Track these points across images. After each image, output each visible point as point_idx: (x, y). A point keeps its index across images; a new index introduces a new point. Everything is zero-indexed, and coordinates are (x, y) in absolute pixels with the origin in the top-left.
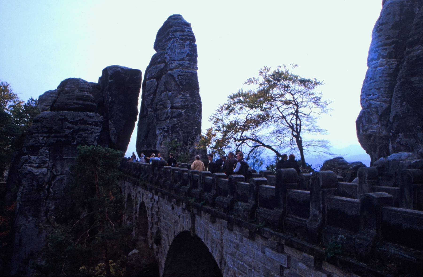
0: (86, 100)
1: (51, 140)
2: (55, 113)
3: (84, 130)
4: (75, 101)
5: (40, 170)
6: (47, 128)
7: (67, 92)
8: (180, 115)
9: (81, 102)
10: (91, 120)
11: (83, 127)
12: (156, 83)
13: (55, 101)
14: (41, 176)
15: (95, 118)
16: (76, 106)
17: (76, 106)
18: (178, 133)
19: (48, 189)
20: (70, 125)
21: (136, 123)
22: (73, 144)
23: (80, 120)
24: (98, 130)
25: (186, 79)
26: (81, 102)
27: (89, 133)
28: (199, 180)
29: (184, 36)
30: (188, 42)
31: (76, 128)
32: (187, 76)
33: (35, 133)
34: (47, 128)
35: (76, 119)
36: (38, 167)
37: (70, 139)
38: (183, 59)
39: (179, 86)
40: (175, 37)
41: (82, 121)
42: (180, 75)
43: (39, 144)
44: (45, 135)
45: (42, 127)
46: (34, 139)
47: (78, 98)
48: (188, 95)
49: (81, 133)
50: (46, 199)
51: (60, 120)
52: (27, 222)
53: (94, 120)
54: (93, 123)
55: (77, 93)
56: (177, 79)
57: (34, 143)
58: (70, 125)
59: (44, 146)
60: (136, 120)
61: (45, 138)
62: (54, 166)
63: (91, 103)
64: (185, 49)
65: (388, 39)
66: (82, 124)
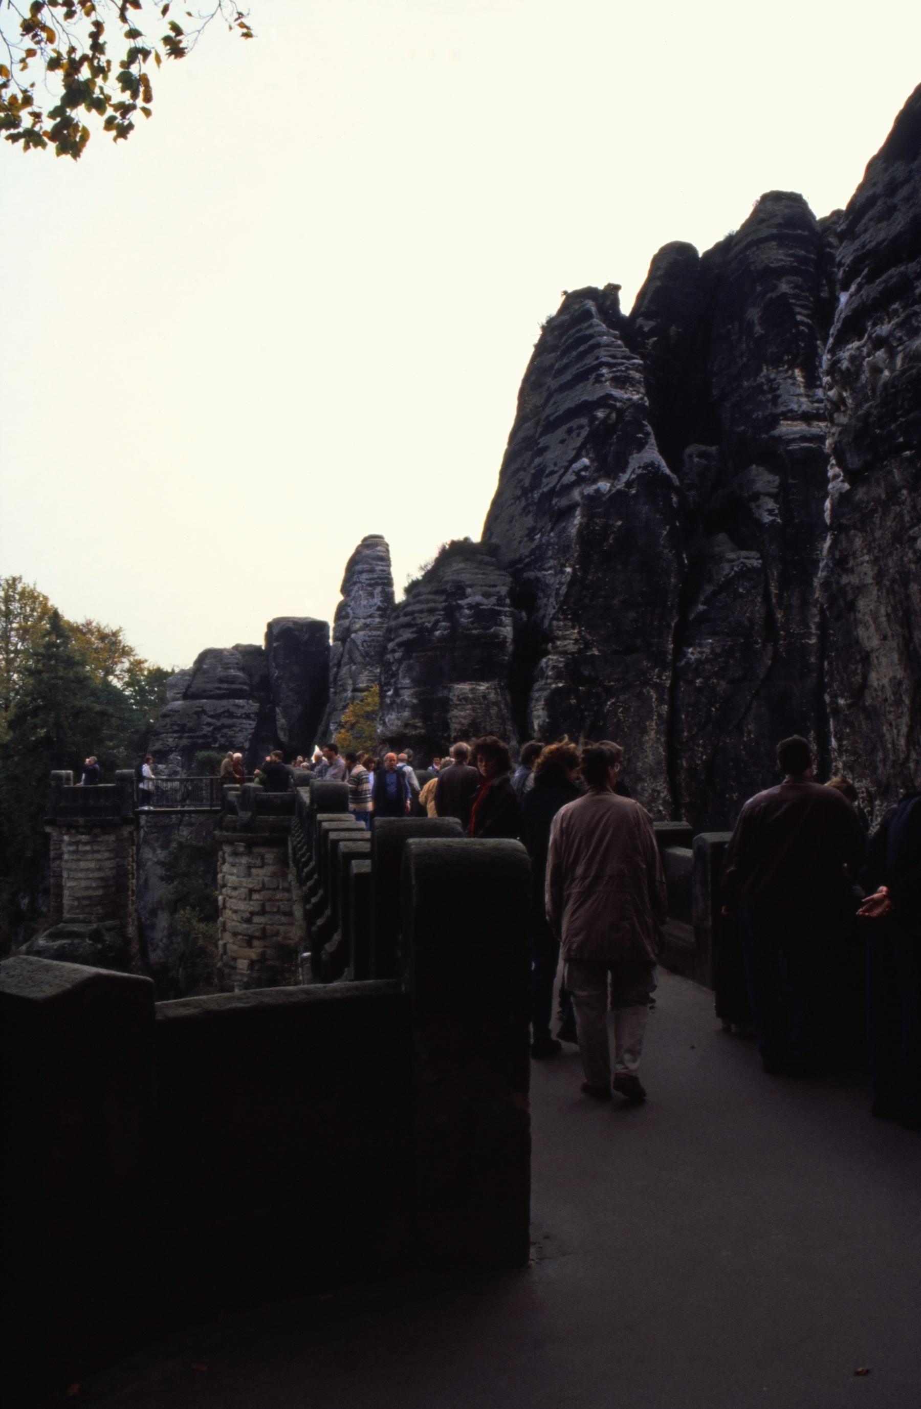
0: (233, 682)
1: (185, 742)
2: (188, 703)
3: (229, 726)
4: (217, 685)
5: (169, 784)
6: (178, 725)
7: (205, 672)
9: (225, 686)
10: (240, 712)
12: (341, 649)
13: (189, 686)
15: (246, 707)
16: (218, 692)
17: (218, 692)
20: (210, 720)
23: (223, 713)
24: (250, 725)
25: (375, 647)
26: (225, 686)
27: (237, 729)
29: (373, 579)
30: (378, 589)
31: (218, 723)
32: (378, 641)
34: (178, 725)
35: (219, 711)
37: (210, 740)
38: (371, 616)
39: (364, 657)
40: (360, 582)
41: (227, 714)
42: (365, 641)
44: (175, 735)
45: (172, 725)
46: (161, 742)
47: (221, 681)
49: (225, 730)
50: (179, 825)
51: (197, 713)
53: (244, 711)
55: (220, 672)
56: (361, 648)
58: (210, 720)
63: (241, 686)
64: (375, 600)
66: (228, 717)
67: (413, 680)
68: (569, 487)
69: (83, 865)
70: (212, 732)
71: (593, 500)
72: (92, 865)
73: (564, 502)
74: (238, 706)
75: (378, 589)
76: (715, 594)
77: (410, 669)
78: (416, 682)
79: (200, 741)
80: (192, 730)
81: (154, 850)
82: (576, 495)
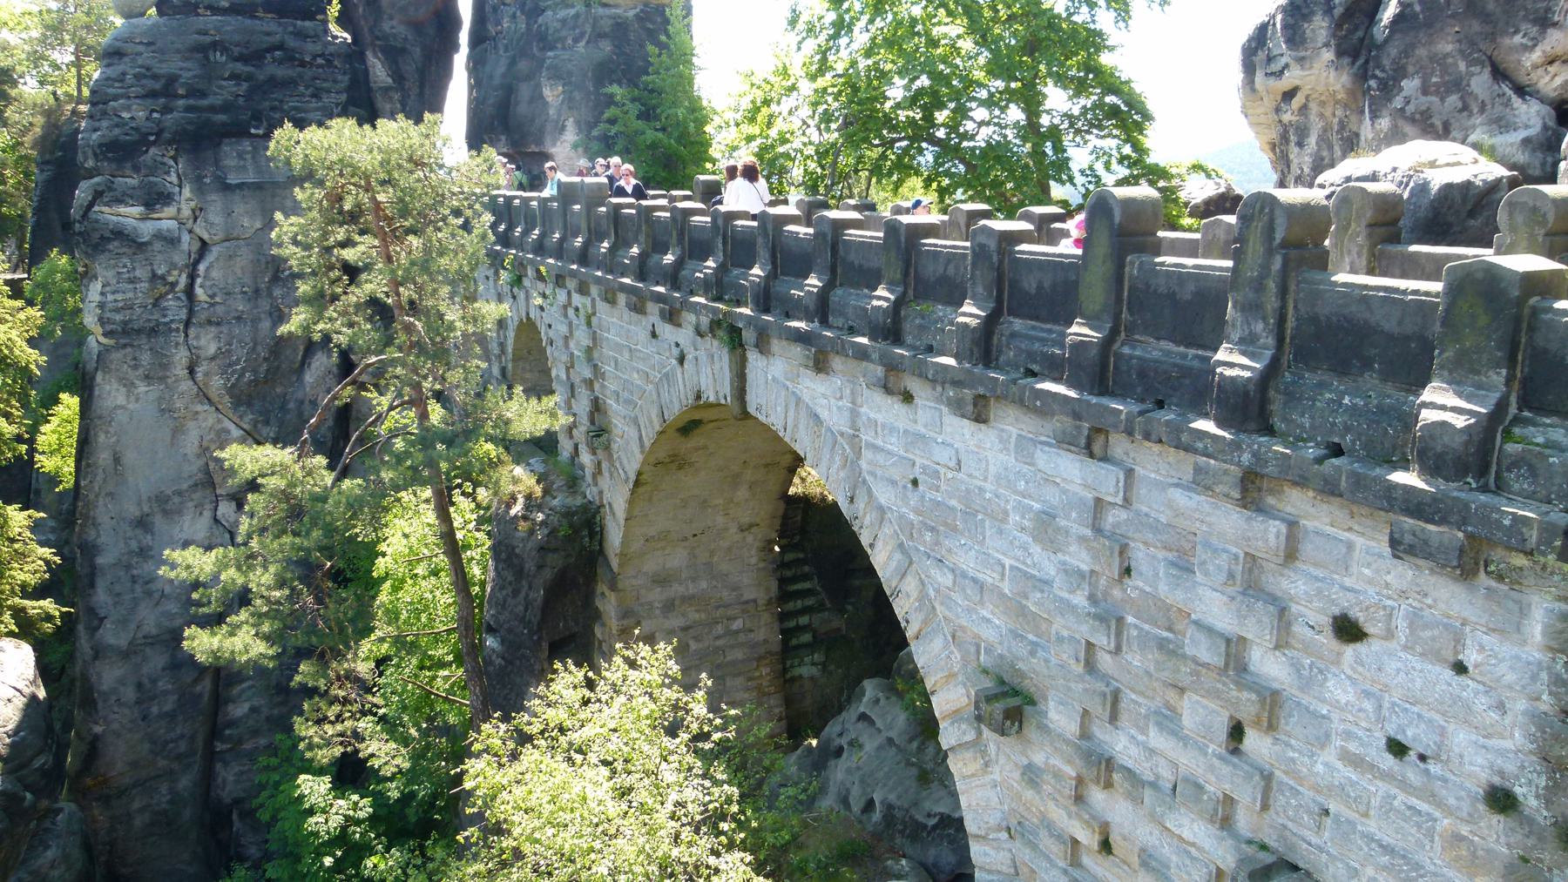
6: (155, 77)
11: (281, 72)
21: (460, 60)
22: (257, 136)
28: (760, 241)
33: (115, 98)
36: (144, 219)
43: (136, 137)
52: (132, 398)
54: (320, 61)
57: (117, 131)
58: (240, 67)
59: (154, 143)
60: (455, 47)
61: (155, 115)
66: (281, 62)
70: (249, 96)
74: (301, 35)
79: (222, 117)
80: (193, 92)
81: (130, 386)
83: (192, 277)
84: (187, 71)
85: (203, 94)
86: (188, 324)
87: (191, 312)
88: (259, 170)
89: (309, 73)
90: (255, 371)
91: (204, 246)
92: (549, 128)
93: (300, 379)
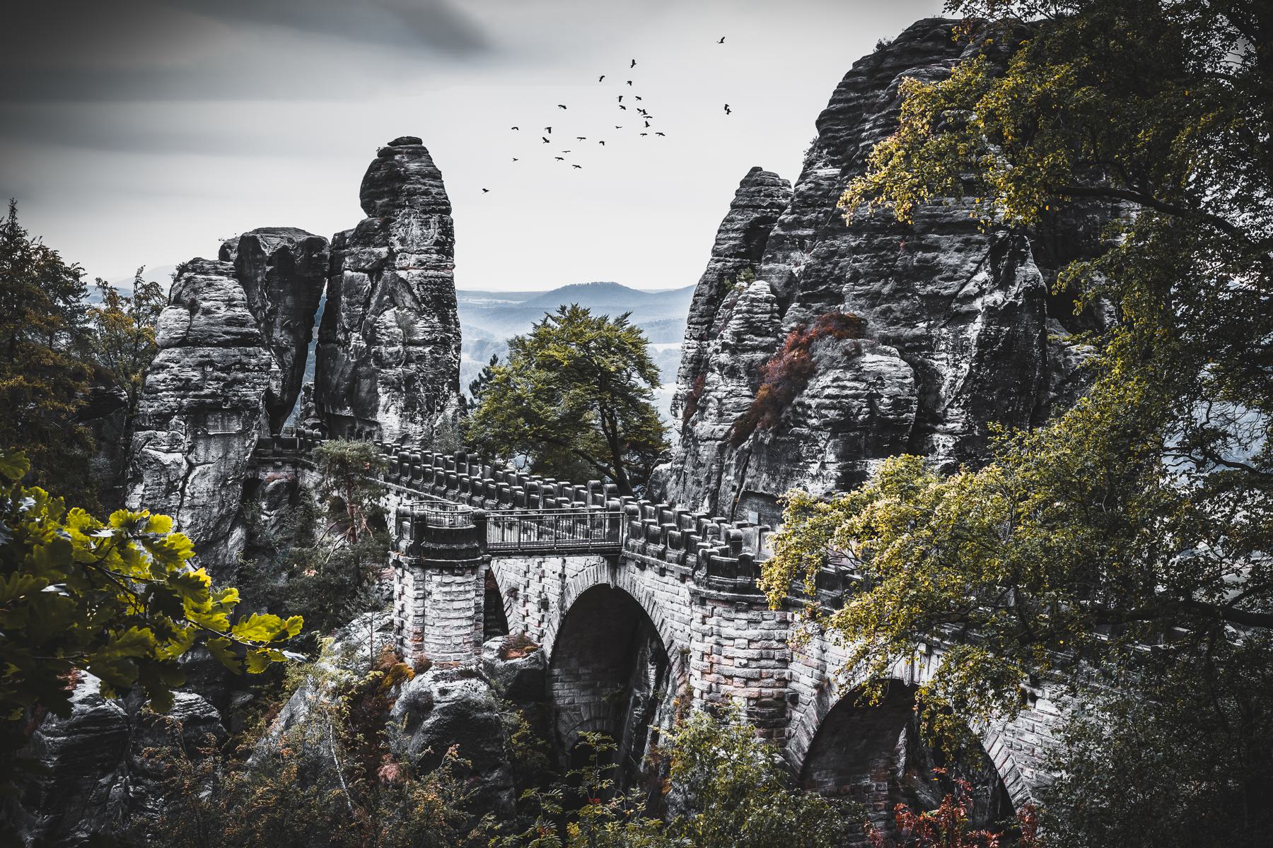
6: (180, 380)
7: (207, 312)
8: (421, 358)
9: (234, 329)
11: (241, 375)
14: (173, 467)
18: (418, 391)
19: (182, 490)
25: (432, 291)
26: (234, 329)
30: (436, 217)
32: (435, 283)
36: (168, 452)
39: (419, 304)
48: (436, 320)
50: (180, 507)
56: (415, 291)
62: (192, 449)
65: (701, 316)
67: (837, 457)
68: (970, 298)
69: (456, 605)
70: (223, 391)
71: (991, 311)
72: (463, 604)
73: (965, 308)
74: (248, 355)
75: (436, 217)
76: (1063, 383)
77: (835, 445)
78: (839, 457)
82: (978, 304)
83: (185, 483)
84: (195, 376)
85: (202, 389)
86: (180, 507)
87: (182, 502)
88: (224, 428)
89: (251, 375)
90: (207, 536)
91: (191, 467)
92: (381, 408)
93: (226, 542)
